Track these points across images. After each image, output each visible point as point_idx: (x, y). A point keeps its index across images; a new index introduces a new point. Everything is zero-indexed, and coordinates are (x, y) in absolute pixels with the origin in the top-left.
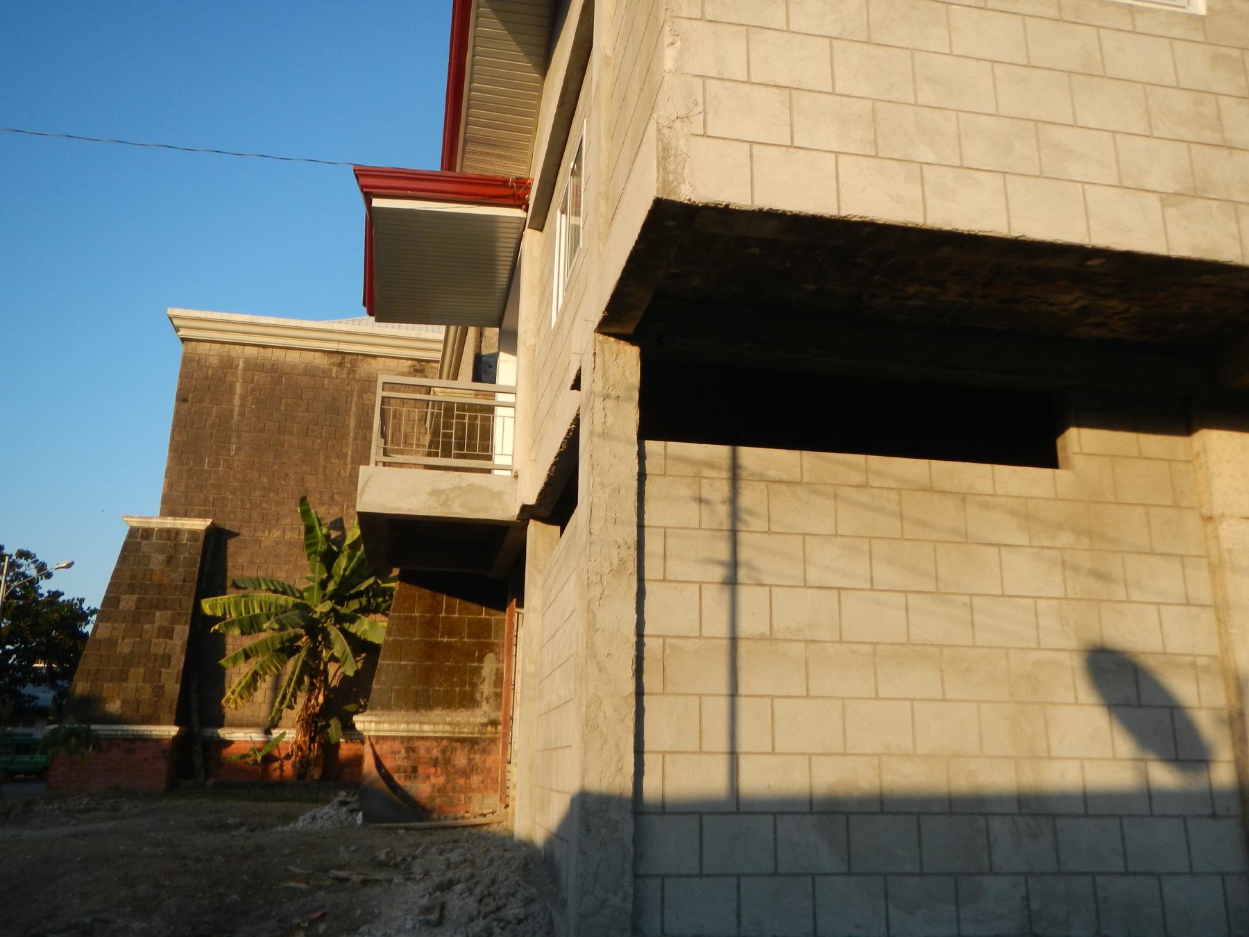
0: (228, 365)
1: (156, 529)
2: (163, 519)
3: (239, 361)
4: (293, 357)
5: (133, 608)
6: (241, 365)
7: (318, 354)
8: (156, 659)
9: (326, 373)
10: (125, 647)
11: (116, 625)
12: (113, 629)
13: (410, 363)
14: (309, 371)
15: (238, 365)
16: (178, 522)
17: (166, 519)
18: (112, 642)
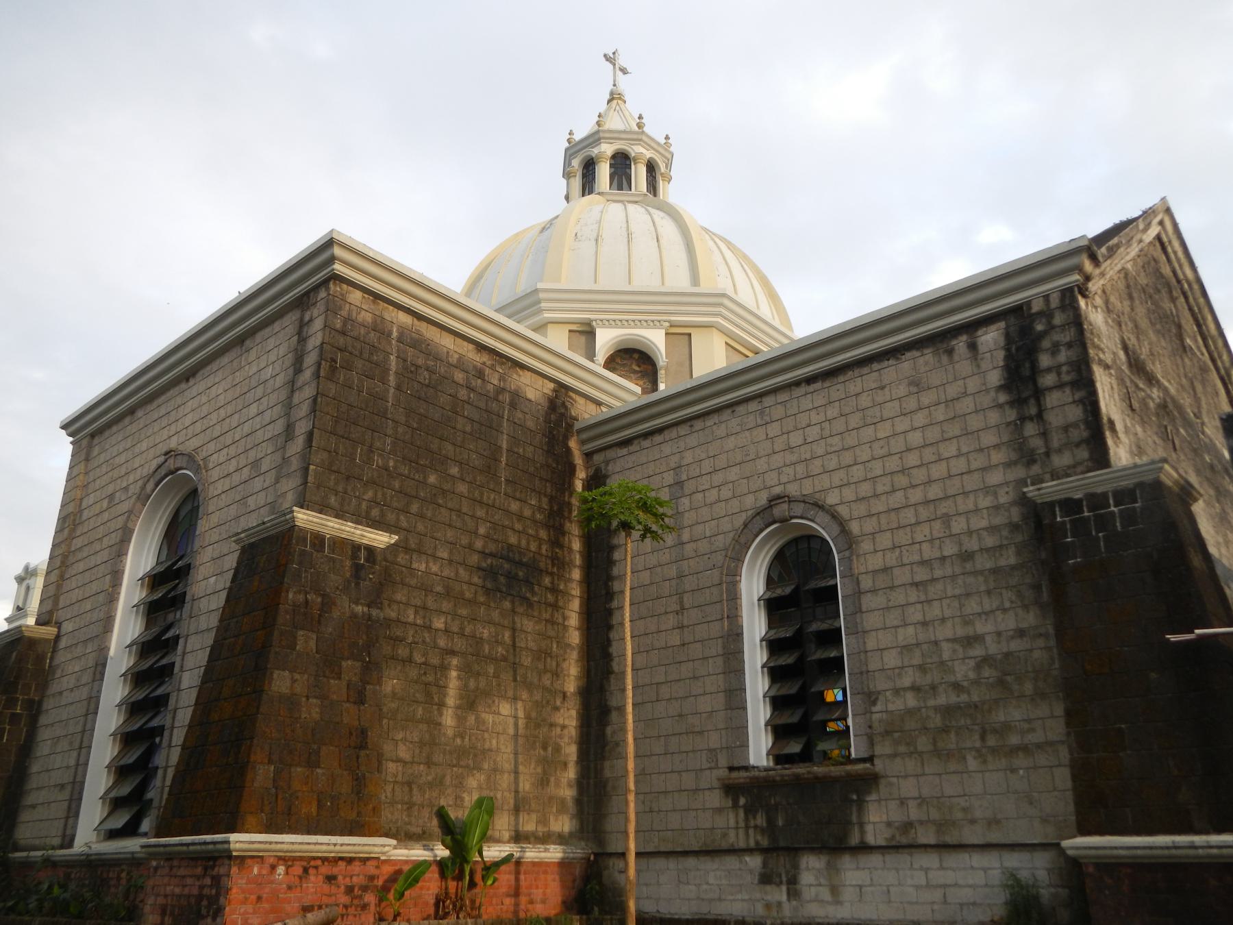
0: (380, 327)
1: (328, 536)
2: (342, 524)
3: (392, 327)
4: (447, 342)
5: (314, 651)
6: (395, 334)
7: (471, 347)
8: (351, 734)
9: (480, 374)
10: (311, 711)
11: (297, 676)
12: (294, 681)
13: (552, 385)
14: (461, 365)
15: (390, 334)
16: (358, 532)
17: (346, 525)
18: (291, 702)
